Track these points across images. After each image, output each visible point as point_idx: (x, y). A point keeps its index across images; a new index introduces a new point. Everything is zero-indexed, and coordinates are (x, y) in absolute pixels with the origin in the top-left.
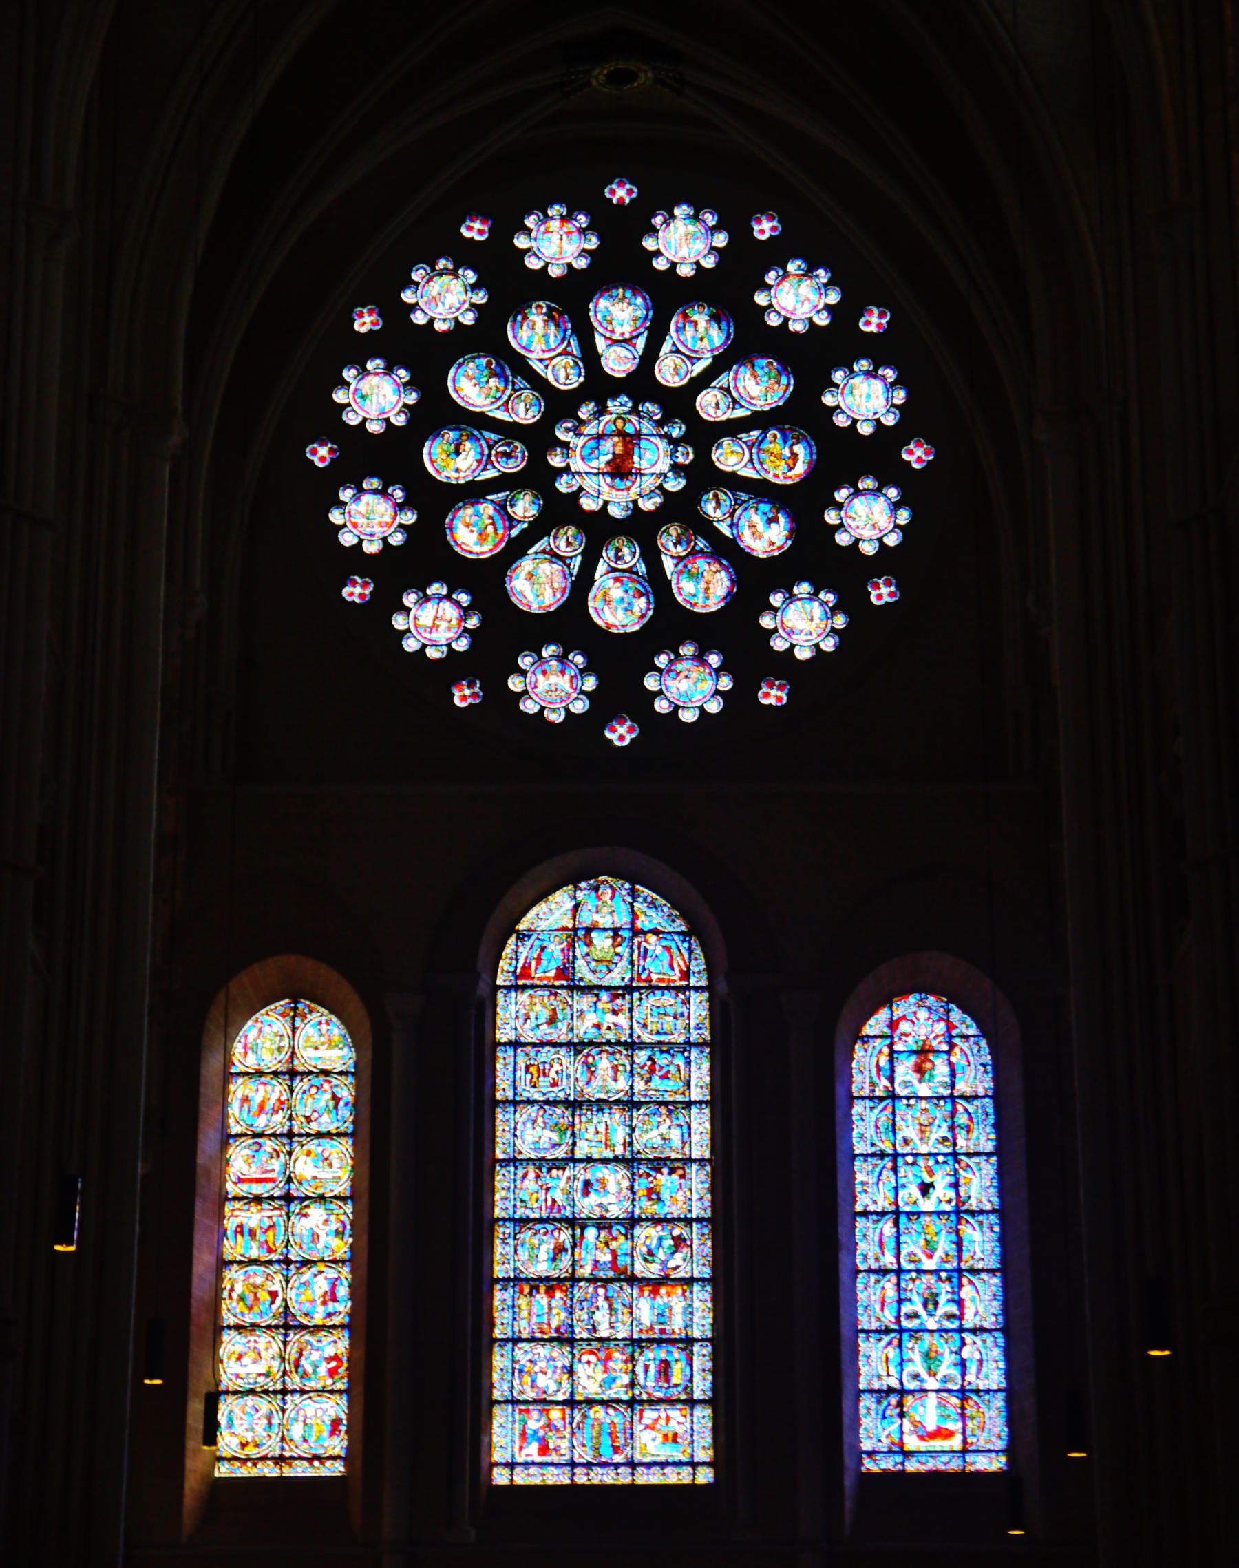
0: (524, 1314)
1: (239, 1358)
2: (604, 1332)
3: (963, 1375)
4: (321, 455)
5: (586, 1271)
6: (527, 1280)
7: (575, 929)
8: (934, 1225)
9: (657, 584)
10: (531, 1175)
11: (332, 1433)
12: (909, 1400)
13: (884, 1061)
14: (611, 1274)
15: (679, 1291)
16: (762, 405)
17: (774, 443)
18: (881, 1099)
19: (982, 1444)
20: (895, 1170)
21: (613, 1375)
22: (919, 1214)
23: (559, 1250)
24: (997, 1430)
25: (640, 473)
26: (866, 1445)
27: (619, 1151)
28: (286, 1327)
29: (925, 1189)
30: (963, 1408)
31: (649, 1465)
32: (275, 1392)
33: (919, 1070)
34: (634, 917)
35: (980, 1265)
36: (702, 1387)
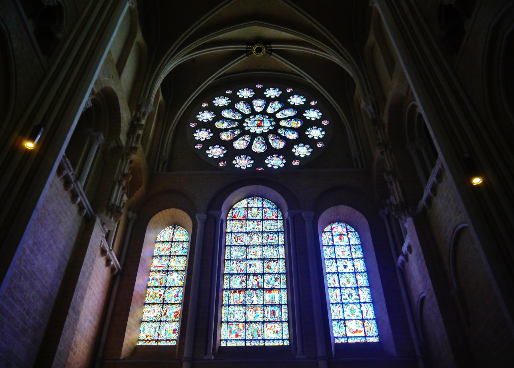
0: (232, 298)
1: (149, 312)
2: (255, 302)
3: (362, 315)
4: (193, 125)
5: (250, 287)
6: (233, 289)
7: (248, 207)
8: (349, 276)
9: (267, 144)
10: (235, 263)
11: (173, 333)
12: (347, 322)
13: (330, 237)
14: (257, 287)
15: (277, 291)
16: (289, 115)
17: (293, 121)
18: (330, 246)
19: (371, 335)
20: (336, 262)
21: (258, 314)
22: (344, 273)
23: (242, 281)
24: (375, 330)
25: (263, 126)
26: (336, 335)
27: (259, 257)
28: (163, 304)
29: (345, 267)
30: (363, 324)
31: (269, 340)
32: (158, 321)
33: (340, 239)
34: (263, 205)
35: (363, 286)
36: (285, 317)
